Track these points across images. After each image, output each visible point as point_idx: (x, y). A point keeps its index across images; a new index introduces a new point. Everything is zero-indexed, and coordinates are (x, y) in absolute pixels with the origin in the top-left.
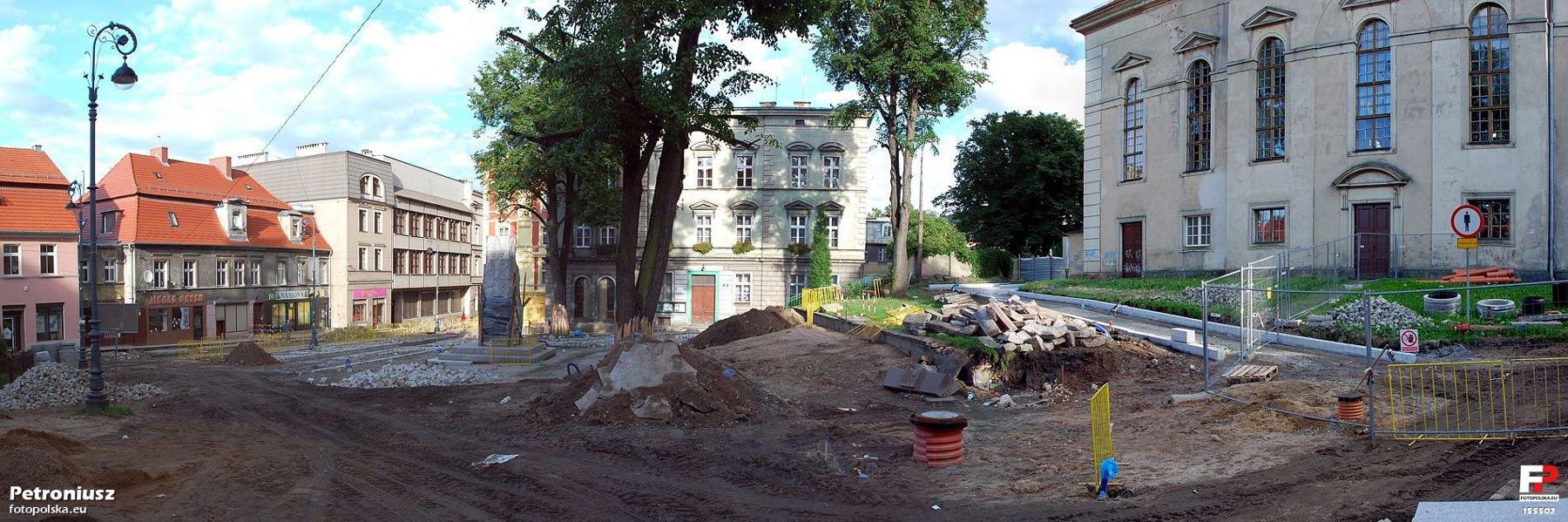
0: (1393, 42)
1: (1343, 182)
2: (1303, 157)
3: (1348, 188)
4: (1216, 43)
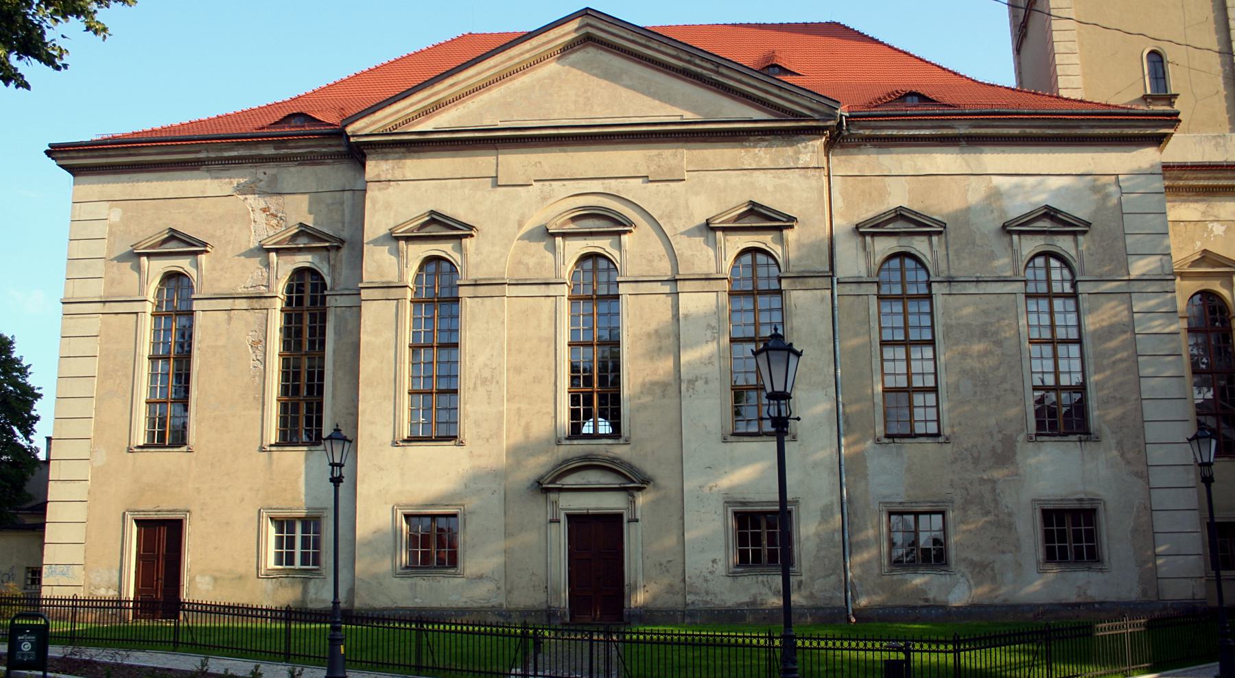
0: (623, 289)
1: (553, 482)
2: (488, 441)
3: (560, 490)
4: (338, 248)
